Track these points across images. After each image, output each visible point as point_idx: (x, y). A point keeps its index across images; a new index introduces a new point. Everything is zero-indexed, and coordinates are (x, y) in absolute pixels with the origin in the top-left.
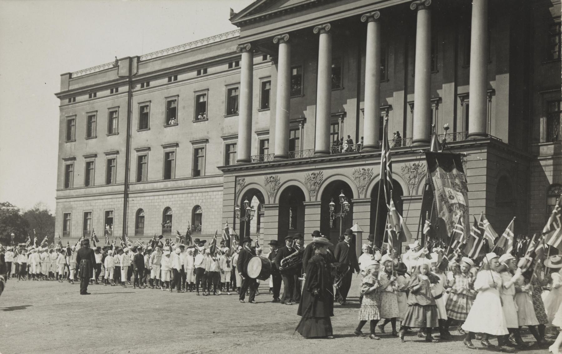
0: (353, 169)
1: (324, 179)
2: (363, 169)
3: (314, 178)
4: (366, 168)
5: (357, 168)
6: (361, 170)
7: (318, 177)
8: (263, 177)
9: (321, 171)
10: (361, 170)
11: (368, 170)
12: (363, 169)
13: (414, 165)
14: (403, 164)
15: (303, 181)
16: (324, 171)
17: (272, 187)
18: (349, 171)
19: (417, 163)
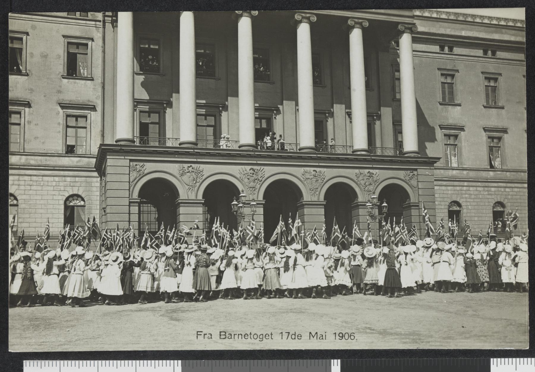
0: (302, 170)
1: (266, 176)
2: (314, 171)
3: (253, 174)
4: (318, 169)
5: (308, 169)
6: (312, 171)
7: (260, 173)
8: (177, 165)
9: (262, 167)
10: (312, 171)
11: (320, 172)
12: (314, 171)
13: (369, 172)
14: (357, 171)
15: (238, 176)
16: (266, 168)
17: (191, 178)
18: (299, 171)
19: (371, 171)
